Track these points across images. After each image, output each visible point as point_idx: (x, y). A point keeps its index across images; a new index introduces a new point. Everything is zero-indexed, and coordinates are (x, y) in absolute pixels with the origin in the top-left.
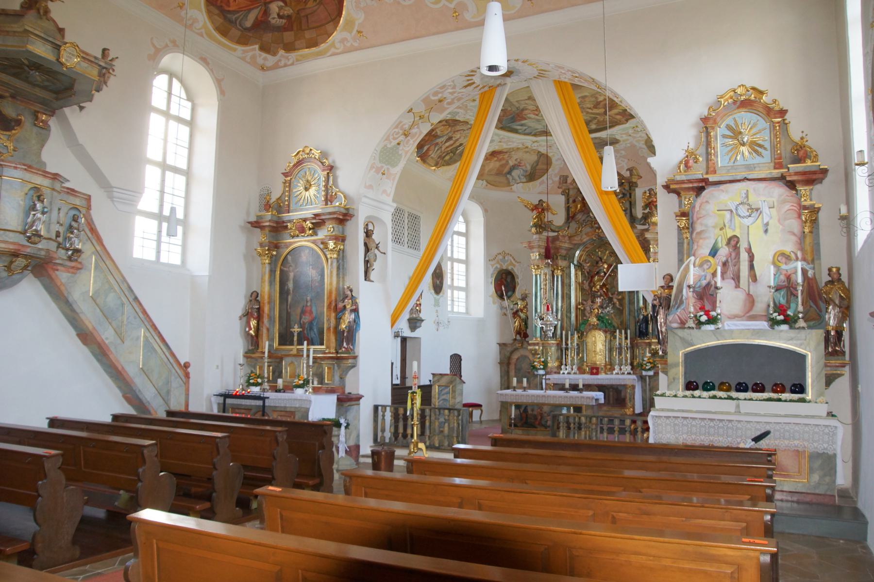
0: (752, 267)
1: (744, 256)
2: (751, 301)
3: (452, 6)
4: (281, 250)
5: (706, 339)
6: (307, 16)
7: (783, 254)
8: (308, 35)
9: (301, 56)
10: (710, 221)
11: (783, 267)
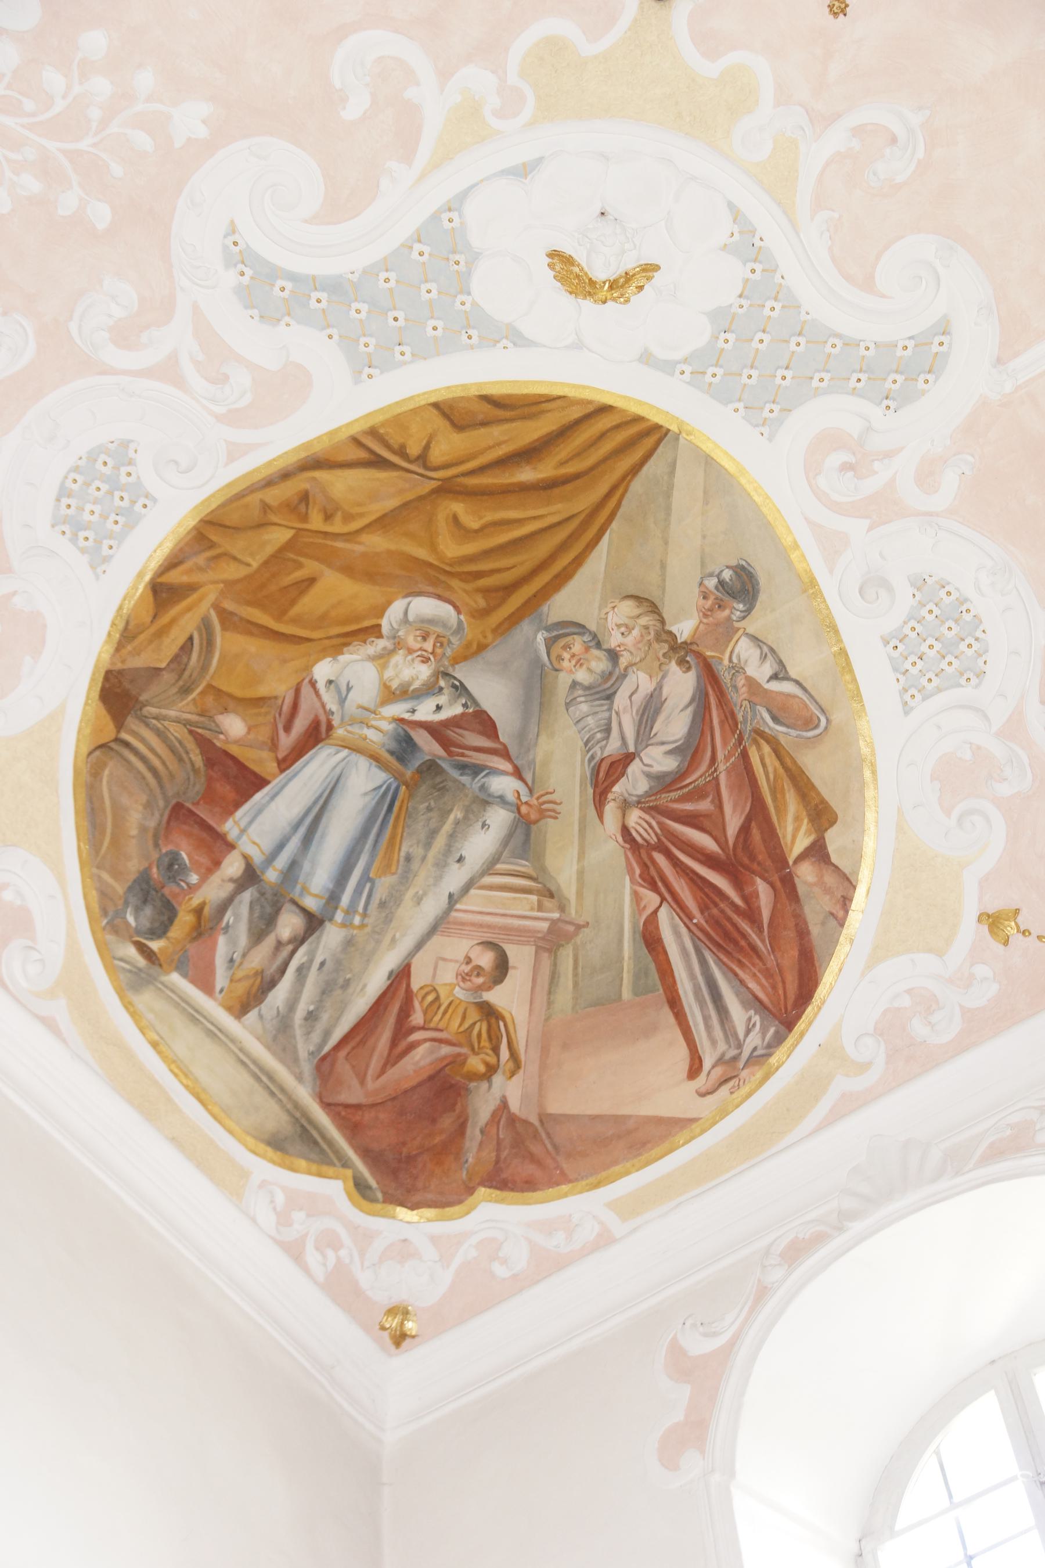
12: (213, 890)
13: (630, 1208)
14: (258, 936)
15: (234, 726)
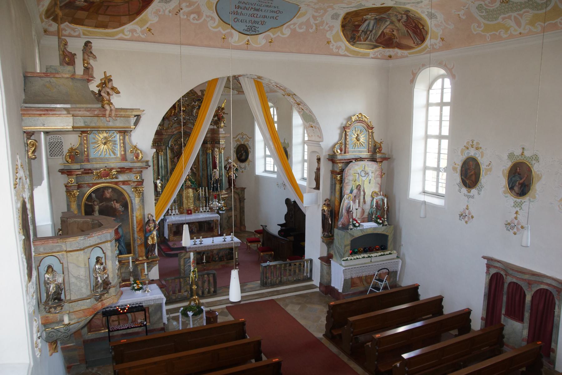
0: (364, 198)
1: (362, 193)
2: (363, 211)
3: (224, 32)
4: (83, 189)
5: (357, 233)
6: (108, 6)
7: (375, 193)
8: (101, 18)
9: (89, 31)
10: (351, 178)
11: (376, 198)
12: (359, 34)
13: (410, 54)
14: (365, 35)
15: (357, 23)
